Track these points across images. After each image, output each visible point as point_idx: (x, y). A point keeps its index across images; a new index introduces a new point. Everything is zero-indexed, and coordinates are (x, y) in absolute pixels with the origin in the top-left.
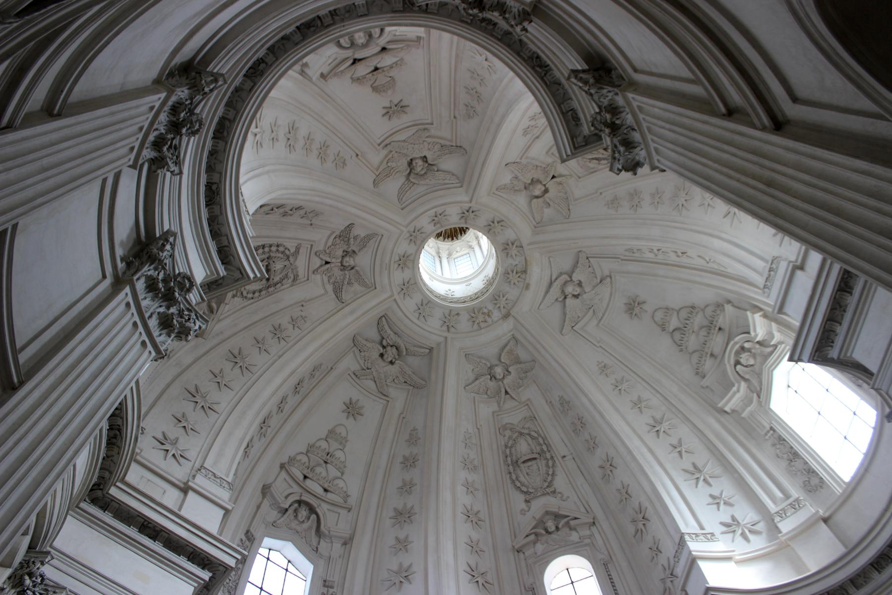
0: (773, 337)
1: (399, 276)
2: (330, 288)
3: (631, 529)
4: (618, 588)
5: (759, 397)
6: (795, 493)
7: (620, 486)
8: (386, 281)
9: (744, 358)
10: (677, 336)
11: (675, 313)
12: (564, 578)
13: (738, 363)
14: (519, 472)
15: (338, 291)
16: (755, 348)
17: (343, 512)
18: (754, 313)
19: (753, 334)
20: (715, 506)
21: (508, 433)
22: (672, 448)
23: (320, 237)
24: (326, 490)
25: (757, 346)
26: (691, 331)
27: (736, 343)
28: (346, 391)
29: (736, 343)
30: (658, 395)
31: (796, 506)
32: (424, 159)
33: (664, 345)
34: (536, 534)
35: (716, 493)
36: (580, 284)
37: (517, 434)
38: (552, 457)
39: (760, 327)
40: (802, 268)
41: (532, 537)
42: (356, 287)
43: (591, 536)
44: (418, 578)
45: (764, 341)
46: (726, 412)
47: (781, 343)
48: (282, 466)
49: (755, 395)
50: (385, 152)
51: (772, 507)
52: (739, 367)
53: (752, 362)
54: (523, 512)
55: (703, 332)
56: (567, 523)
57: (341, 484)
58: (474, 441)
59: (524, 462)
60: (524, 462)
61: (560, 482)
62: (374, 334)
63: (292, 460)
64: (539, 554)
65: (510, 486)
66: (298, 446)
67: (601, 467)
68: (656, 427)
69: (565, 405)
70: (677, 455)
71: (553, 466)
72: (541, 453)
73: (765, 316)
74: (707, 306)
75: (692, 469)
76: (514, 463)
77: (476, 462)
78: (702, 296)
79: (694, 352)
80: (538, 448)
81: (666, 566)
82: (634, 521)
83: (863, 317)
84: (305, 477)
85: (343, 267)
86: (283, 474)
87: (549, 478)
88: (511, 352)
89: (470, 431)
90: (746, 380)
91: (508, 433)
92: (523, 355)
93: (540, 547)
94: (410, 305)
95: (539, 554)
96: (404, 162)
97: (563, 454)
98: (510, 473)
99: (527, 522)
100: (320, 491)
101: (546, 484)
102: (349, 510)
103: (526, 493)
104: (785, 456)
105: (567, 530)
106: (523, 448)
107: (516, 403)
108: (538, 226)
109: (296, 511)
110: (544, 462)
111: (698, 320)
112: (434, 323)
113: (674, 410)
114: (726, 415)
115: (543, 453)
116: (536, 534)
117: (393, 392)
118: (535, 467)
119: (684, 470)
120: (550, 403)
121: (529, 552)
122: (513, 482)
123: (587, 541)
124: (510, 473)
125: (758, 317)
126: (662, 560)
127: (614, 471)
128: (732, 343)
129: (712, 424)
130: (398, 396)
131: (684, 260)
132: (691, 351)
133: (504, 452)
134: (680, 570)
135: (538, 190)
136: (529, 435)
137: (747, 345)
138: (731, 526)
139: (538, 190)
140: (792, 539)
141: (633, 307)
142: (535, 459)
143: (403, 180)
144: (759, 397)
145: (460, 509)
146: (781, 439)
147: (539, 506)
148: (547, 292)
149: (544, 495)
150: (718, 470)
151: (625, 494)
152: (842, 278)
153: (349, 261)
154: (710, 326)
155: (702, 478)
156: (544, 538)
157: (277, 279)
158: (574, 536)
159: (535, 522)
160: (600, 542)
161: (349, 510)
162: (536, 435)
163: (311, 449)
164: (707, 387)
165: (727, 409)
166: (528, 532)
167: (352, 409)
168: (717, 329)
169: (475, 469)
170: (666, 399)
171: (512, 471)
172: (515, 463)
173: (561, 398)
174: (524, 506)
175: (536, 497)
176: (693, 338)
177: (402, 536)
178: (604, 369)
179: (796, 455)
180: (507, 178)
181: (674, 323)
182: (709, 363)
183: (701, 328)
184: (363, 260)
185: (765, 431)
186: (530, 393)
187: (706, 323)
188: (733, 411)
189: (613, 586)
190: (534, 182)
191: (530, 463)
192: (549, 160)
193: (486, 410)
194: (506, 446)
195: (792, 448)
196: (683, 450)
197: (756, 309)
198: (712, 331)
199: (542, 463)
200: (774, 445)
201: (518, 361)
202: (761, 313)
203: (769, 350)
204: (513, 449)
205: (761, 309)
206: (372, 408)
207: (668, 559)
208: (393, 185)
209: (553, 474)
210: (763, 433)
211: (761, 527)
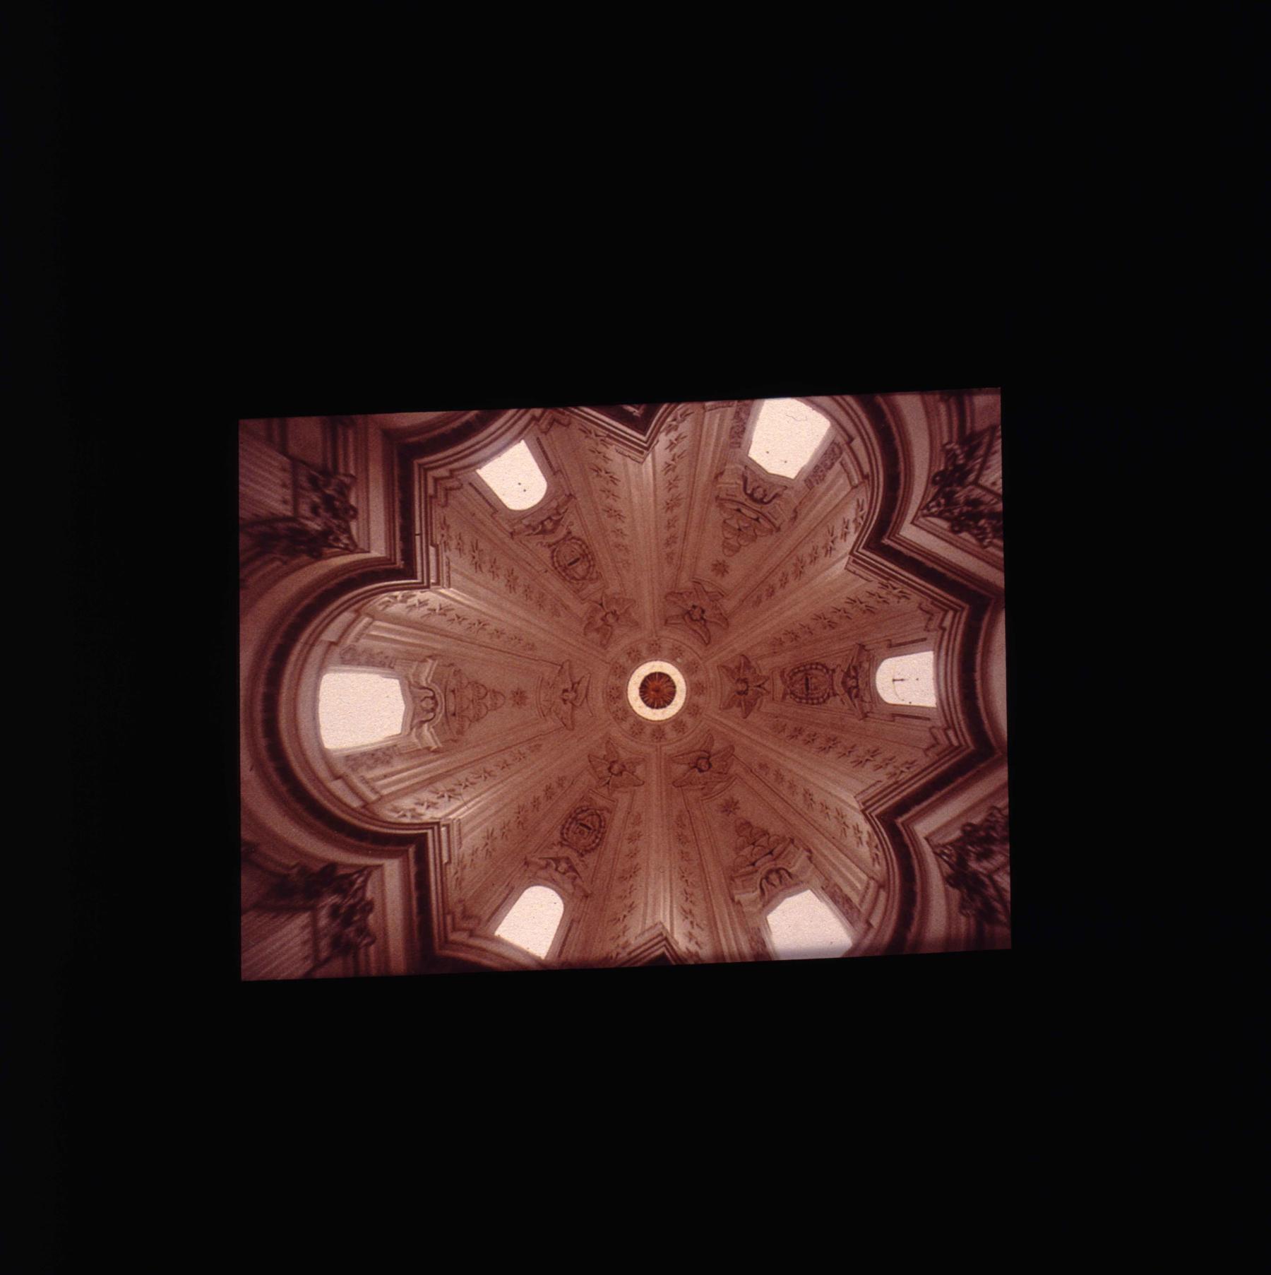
1: (700, 677)
2: (753, 663)
3: (481, 546)
8: (711, 675)
15: (747, 664)
17: (723, 495)
21: (594, 575)
23: (767, 706)
24: (739, 510)
28: (727, 582)
32: (701, 771)
33: (489, 677)
34: (558, 514)
36: (564, 701)
42: (732, 666)
43: (513, 525)
44: (659, 468)
48: (778, 529)
50: (732, 771)
51: (378, 623)
57: (725, 515)
61: (546, 554)
62: (712, 629)
63: (771, 532)
66: (766, 541)
68: (482, 624)
69: (556, 613)
76: (586, 555)
84: (757, 520)
85: (745, 681)
86: (777, 523)
88: (604, 635)
89: (624, 572)
91: (594, 575)
92: (595, 636)
93: (554, 504)
94: (689, 656)
96: (715, 766)
100: (744, 510)
102: (717, 498)
105: (534, 524)
106: (580, 569)
107: (593, 598)
108: (608, 741)
109: (765, 495)
112: (666, 645)
115: (563, 570)
116: (558, 514)
117: (690, 584)
120: (567, 607)
126: (453, 544)
130: (685, 582)
135: (616, 768)
139: (616, 768)
141: (519, 697)
143: (713, 751)
145: (627, 520)
147: (562, 532)
148: (587, 689)
149: (557, 542)
153: (741, 687)
157: (800, 675)
158: (525, 522)
161: (717, 498)
163: (754, 538)
167: (721, 568)
169: (617, 546)
173: (559, 616)
174: (571, 528)
175: (564, 539)
177: (673, 491)
178: (532, 647)
180: (639, 770)
184: (729, 687)
186: (581, 609)
190: (621, 773)
192: (616, 795)
193: (614, 588)
201: (598, 630)
206: (704, 570)
208: (717, 746)
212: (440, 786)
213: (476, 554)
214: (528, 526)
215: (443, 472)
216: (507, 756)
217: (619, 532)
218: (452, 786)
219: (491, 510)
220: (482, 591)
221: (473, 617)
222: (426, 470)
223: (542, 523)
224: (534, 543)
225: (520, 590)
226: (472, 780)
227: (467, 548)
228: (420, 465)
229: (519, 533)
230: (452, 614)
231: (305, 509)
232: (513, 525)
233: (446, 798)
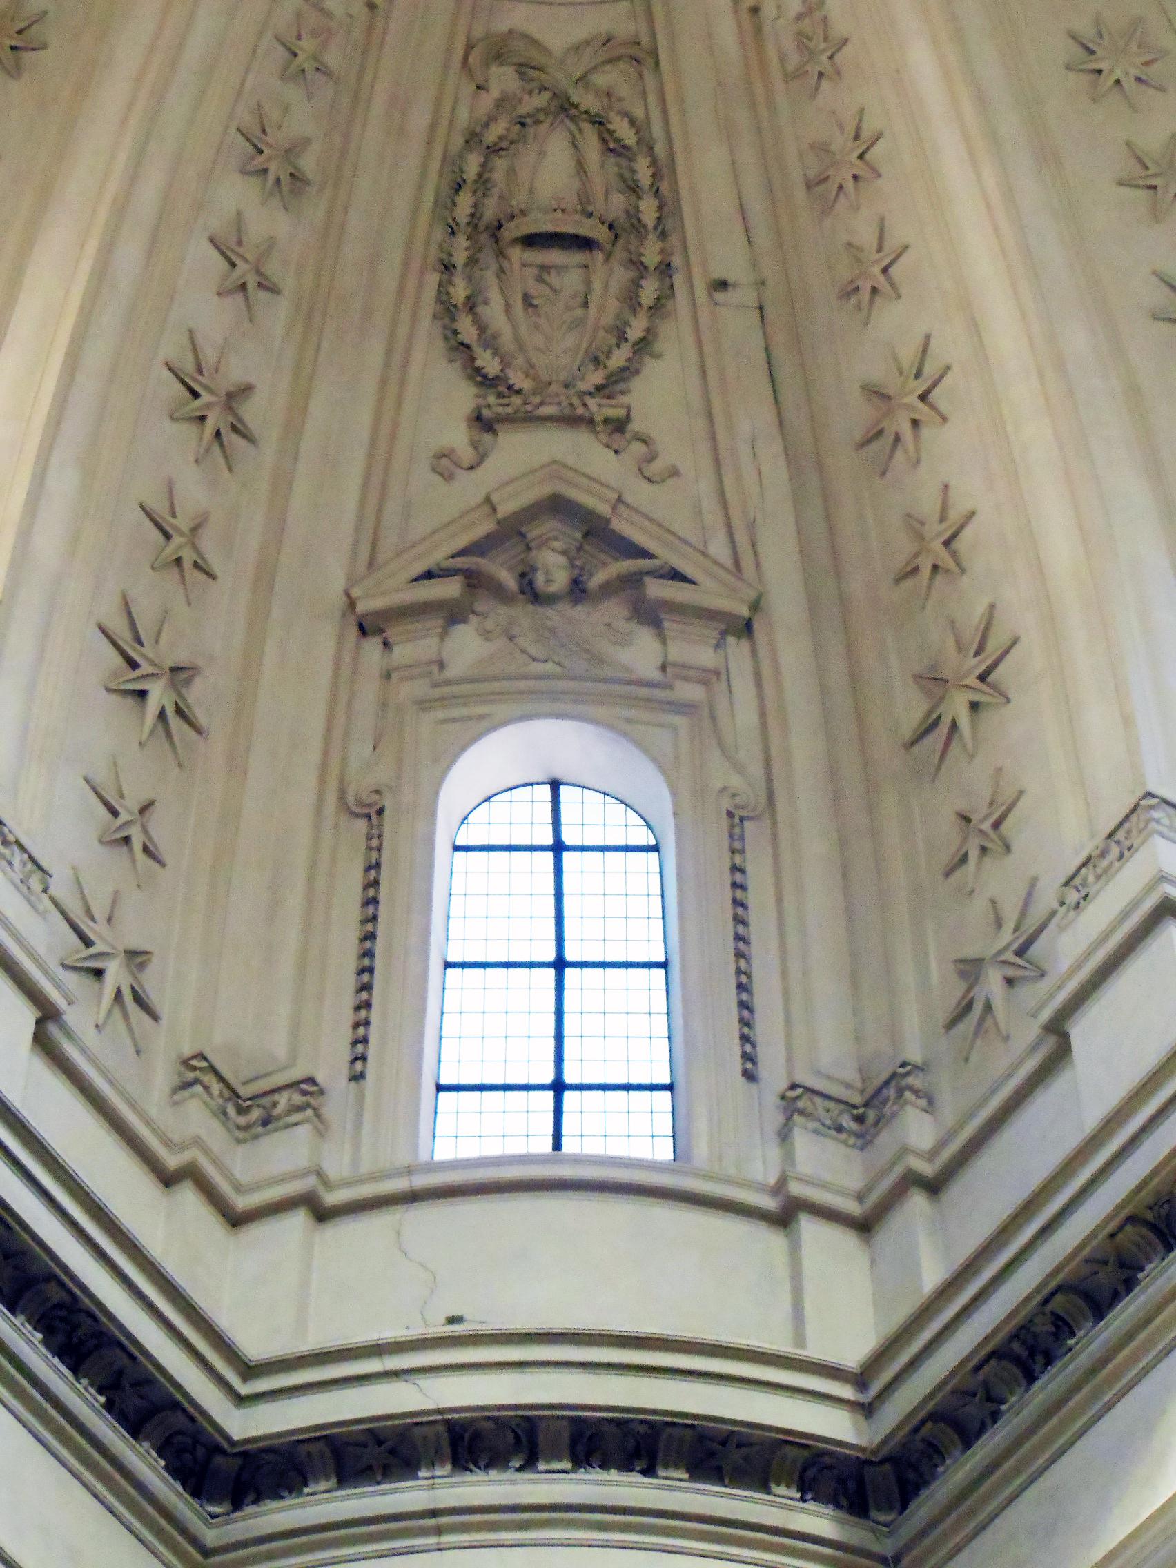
3: (910, 708)
4: (754, 933)
7: (928, 505)
12: (528, 816)
14: (490, 275)
34: (475, 581)
37: (541, 100)
38: (665, 269)
41: (450, 589)
54: (445, 464)
56: (632, 581)
58: (333, 58)
59: (531, 241)
60: (531, 241)
61: (660, 395)
64: (452, 672)
65: (426, 323)
67: (875, 393)
71: (657, 308)
72: (625, 229)
76: (480, 231)
77: (308, 164)
80: (618, 202)
82: (934, 682)
87: (619, 358)
91: (503, 79)
93: (467, 646)
95: (452, 672)
97: (718, 274)
98: (447, 267)
99: (444, 513)
101: (597, 377)
103: (485, 381)
105: (614, 610)
106: (551, 174)
110: (621, 275)
115: (631, 233)
116: (475, 581)
118: (571, 281)
121: (413, 647)
122: (447, 310)
123: (689, 692)
124: (447, 267)
126: (1000, 882)
127: (925, 432)
133: (452, 163)
134: (1072, 945)
136: (599, 122)
142: (584, 243)
147: (524, 461)
149: (571, 421)
151: (935, 554)
156: (500, 614)
158: (641, 653)
159: (484, 527)
160: (745, 716)
162: (629, 137)
166: (438, 556)
171: (460, 258)
172: (490, 234)
174: (458, 436)
189: (739, 921)
191: (555, 256)
194: (472, 139)
199: (609, 278)
204: (500, 165)
207: (1034, 881)
209: (644, 346)
214: (650, 615)
217: (246, 276)
222: (860, 1379)
223: (578, 590)
224: (667, 512)
225: (898, 326)
227: (970, 780)
228: (867, 1410)
229: (710, 615)
232: (708, 677)
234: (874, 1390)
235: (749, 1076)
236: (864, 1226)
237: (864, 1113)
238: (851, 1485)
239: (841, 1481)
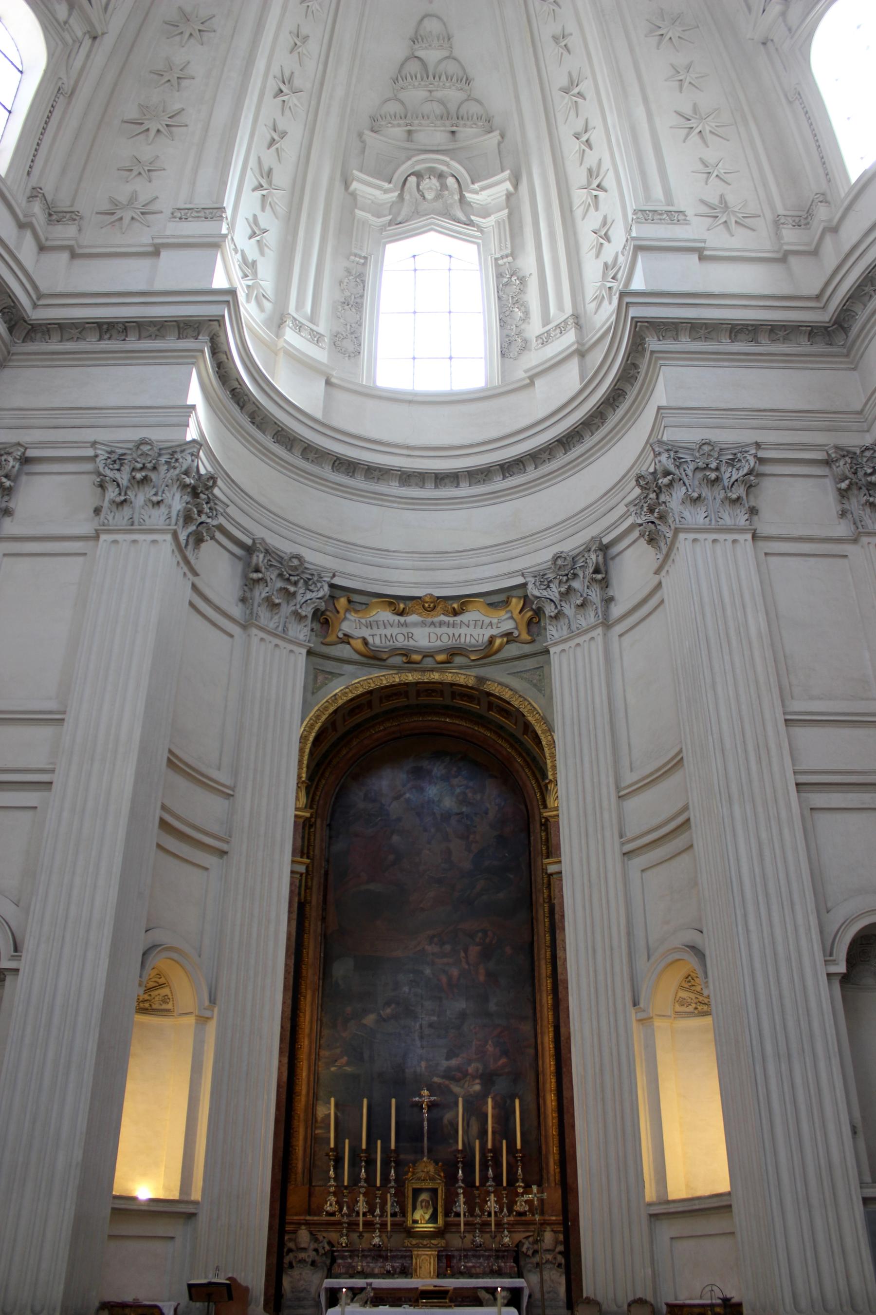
0: (486, 214)
3: (132, 113)
5: (390, 223)
6: (322, 328)
9: (430, 184)
10: (413, 67)
11: (446, 53)
13: (419, 175)
16: (452, 194)
18: (509, 179)
19: (476, 186)
20: (249, 231)
22: (271, 125)
25: (457, 197)
26: (431, 87)
27: (448, 165)
29: (448, 165)
30: (321, 67)
31: (316, 338)
35: (263, 224)
39: (489, 194)
40: (702, 258)
45: (469, 204)
46: (347, 184)
47: (480, 229)
49: (390, 217)
51: (292, 309)
52: (413, 180)
53: (429, 196)
55: (438, 109)
68: (285, 85)
70: (269, 137)
73: (509, 196)
74: (480, 102)
75: (266, 169)
78: (493, 89)
79: (402, 103)
81: (143, 198)
83: (712, 363)
90: (401, 196)
104: (347, 294)
111: (453, 95)
113: (313, 103)
114: (343, 187)
119: (259, 158)
125: (508, 186)
128: (447, 159)
129: (323, 171)
131: (550, 51)
132: (402, 95)
137: (451, 181)
138: (249, 267)
140: (288, 353)
144: (390, 223)
146: (360, 279)
150: (282, 209)
151: (174, 77)
152: (748, 325)
154: (453, 119)
155: (264, 192)
164: (363, 142)
165: (355, 185)
168: (454, 129)
170: (322, 84)
176: (422, 94)
179: (358, 306)
181: (432, 56)
182: (397, 132)
183: (442, 102)
185: (359, 252)
187: (453, 108)
188: (353, 195)
195: (362, 296)
196: (277, 145)
197: (516, 181)
198: (448, 123)
200: (348, 271)
202: (511, 189)
203: (460, 215)
205: (516, 186)
210: (355, 251)
211: (268, 305)
212: (579, 197)
213: (154, 127)
215: (27, 252)
216: (547, 30)
218: (583, 179)
219: (62, 100)
220: (221, 114)
221: (271, 105)
222: (40, 296)
226: (579, 126)
228: (35, 306)
230: (269, 158)
231: (157, 517)
233: (601, 194)
234: (40, 303)
235: (29, 173)
236: (42, 248)
237: (54, 216)
238: (13, 323)
239: (11, 320)
